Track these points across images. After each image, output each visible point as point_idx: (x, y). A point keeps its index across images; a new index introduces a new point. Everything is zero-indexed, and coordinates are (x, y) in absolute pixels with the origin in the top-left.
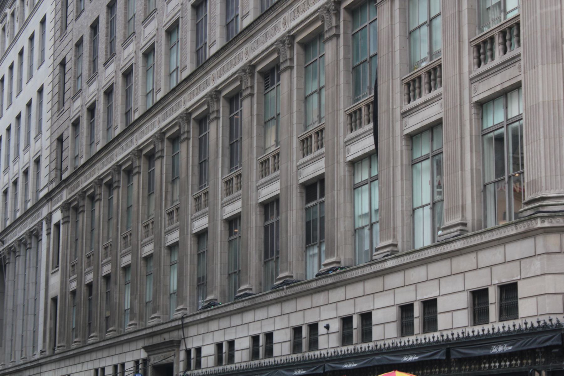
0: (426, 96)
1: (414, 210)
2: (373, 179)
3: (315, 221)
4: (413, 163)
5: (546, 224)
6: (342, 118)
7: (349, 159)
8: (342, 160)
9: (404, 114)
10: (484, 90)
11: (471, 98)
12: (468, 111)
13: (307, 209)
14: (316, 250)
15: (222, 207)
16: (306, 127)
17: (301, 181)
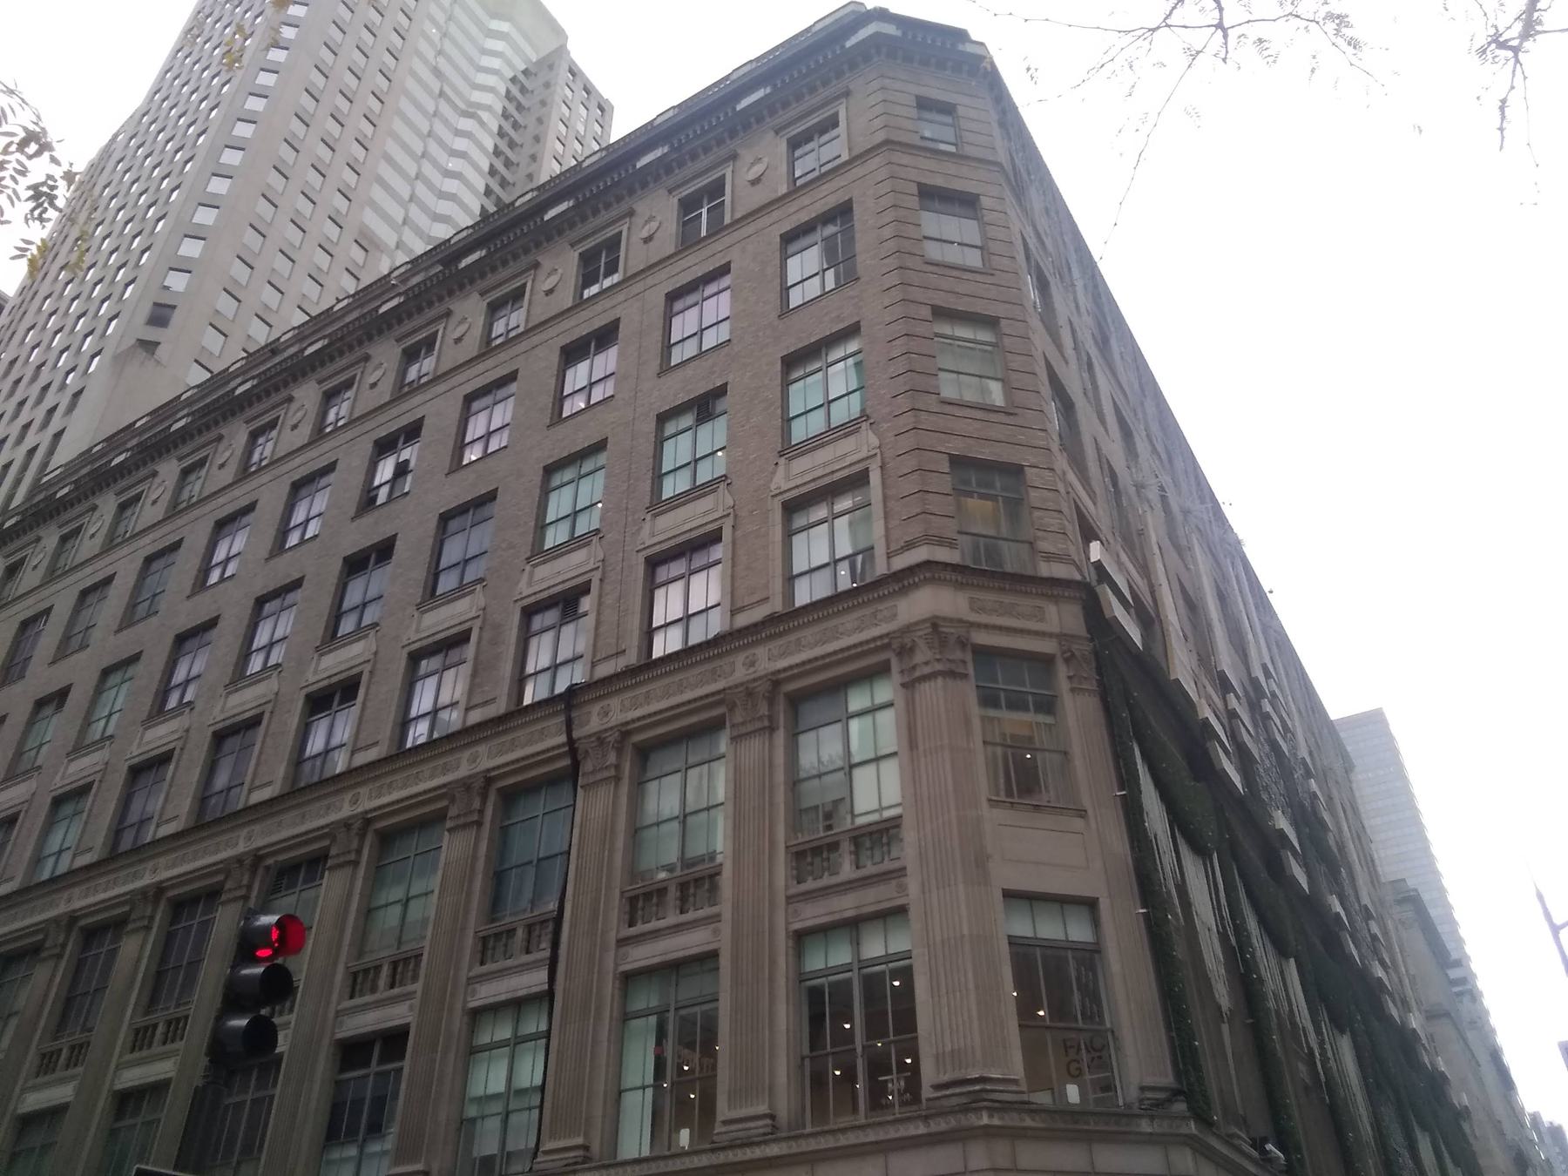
0: (673, 918)
1: (620, 1093)
2: (518, 1041)
3: (358, 1103)
4: (626, 1017)
5: (996, 1122)
6: (469, 941)
7: (472, 1005)
8: (459, 1006)
9: (622, 942)
10: (812, 914)
11: (788, 923)
12: (782, 942)
13: (337, 1083)
14: (352, 1151)
15: (117, 1068)
16: (361, 954)
17: (339, 1036)
